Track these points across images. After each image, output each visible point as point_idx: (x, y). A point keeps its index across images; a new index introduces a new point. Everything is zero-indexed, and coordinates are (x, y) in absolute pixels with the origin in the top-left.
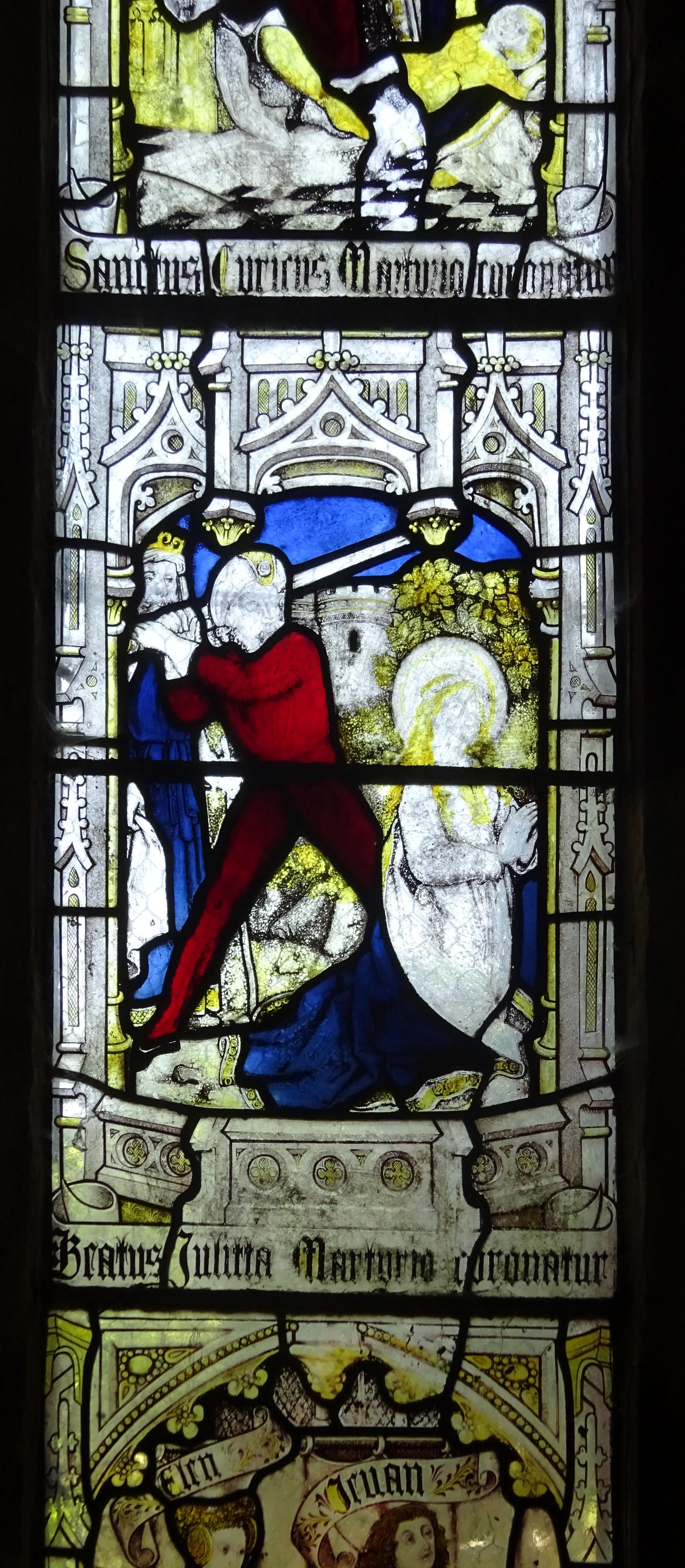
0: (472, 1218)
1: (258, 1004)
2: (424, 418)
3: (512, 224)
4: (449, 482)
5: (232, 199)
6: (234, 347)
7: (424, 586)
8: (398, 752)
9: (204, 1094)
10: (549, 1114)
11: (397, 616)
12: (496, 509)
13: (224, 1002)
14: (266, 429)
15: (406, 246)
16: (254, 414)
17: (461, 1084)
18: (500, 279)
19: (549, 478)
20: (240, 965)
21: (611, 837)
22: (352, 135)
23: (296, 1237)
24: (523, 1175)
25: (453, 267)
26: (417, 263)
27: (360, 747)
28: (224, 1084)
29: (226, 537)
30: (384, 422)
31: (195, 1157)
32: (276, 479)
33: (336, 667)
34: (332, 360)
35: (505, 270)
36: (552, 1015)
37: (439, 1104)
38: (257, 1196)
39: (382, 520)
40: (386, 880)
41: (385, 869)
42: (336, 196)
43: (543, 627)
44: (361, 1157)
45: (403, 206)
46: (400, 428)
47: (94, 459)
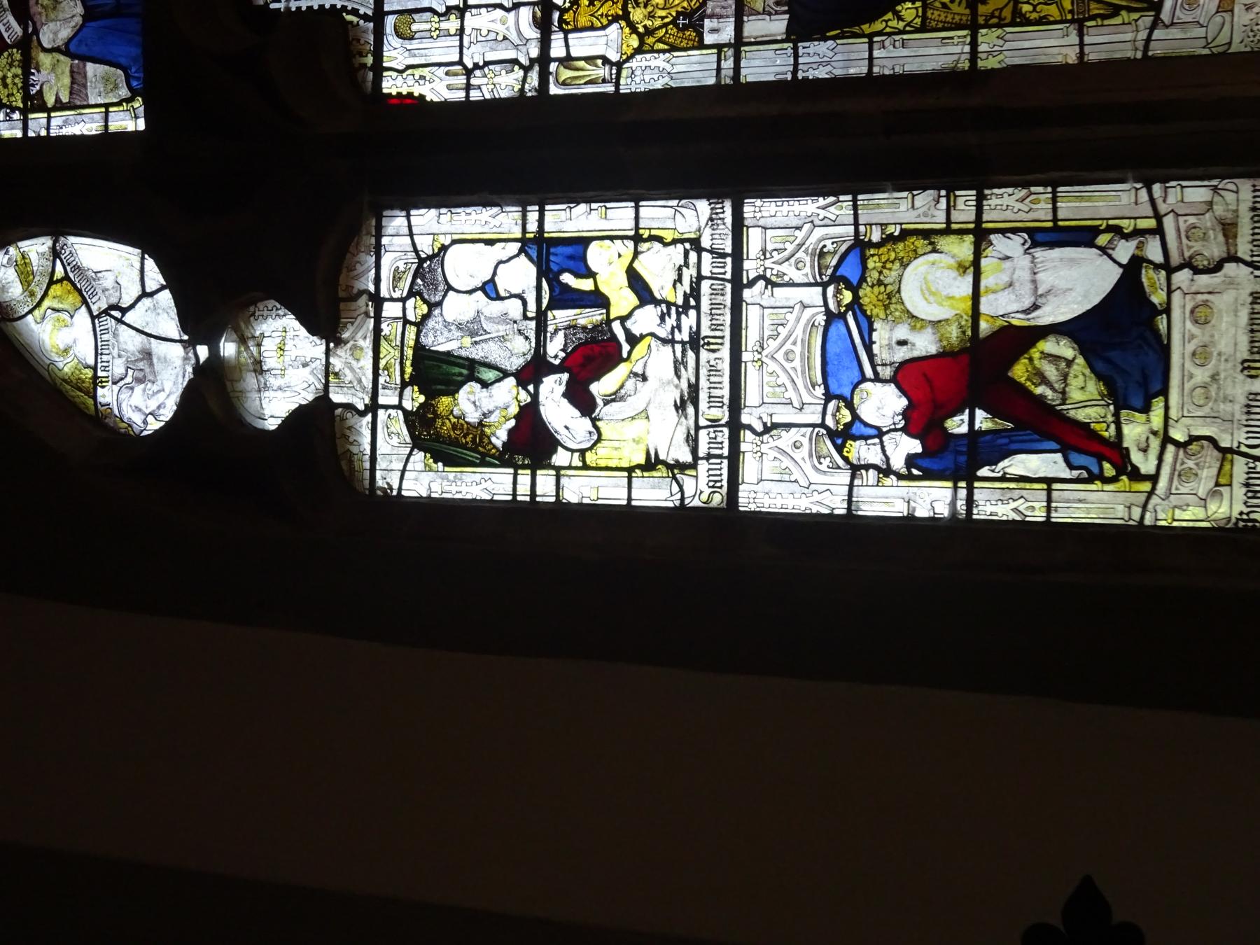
0: (1230, 268)
1: (1103, 400)
2: (787, 304)
3: (693, 256)
4: (820, 289)
5: (680, 411)
6: (750, 412)
7: (874, 303)
8: (962, 317)
9: (1155, 433)
10: (1168, 222)
11: (890, 318)
12: (834, 262)
13: (1101, 420)
14: (791, 394)
15: (703, 315)
16: (784, 401)
17: (1150, 276)
19: (819, 232)
20: (1080, 410)
21: (1010, 190)
22: (649, 345)
23: (1241, 377)
24: (1205, 237)
25: (713, 289)
26: (711, 309)
27: (959, 339)
28: (1148, 421)
29: (846, 416)
30: (788, 327)
31: (1193, 439)
32: (817, 387)
33: (916, 354)
34: (757, 356)
35: (715, 260)
36: (1111, 222)
37: (1162, 290)
38: (1216, 400)
39: (838, 327)
40: (1033, 323)
41: (1026, 324)
42: (679, 355)
43: (896, 234)
44: (1192, 337)
45: (683, 317)
46: (791, 318)
47: (806, 491)
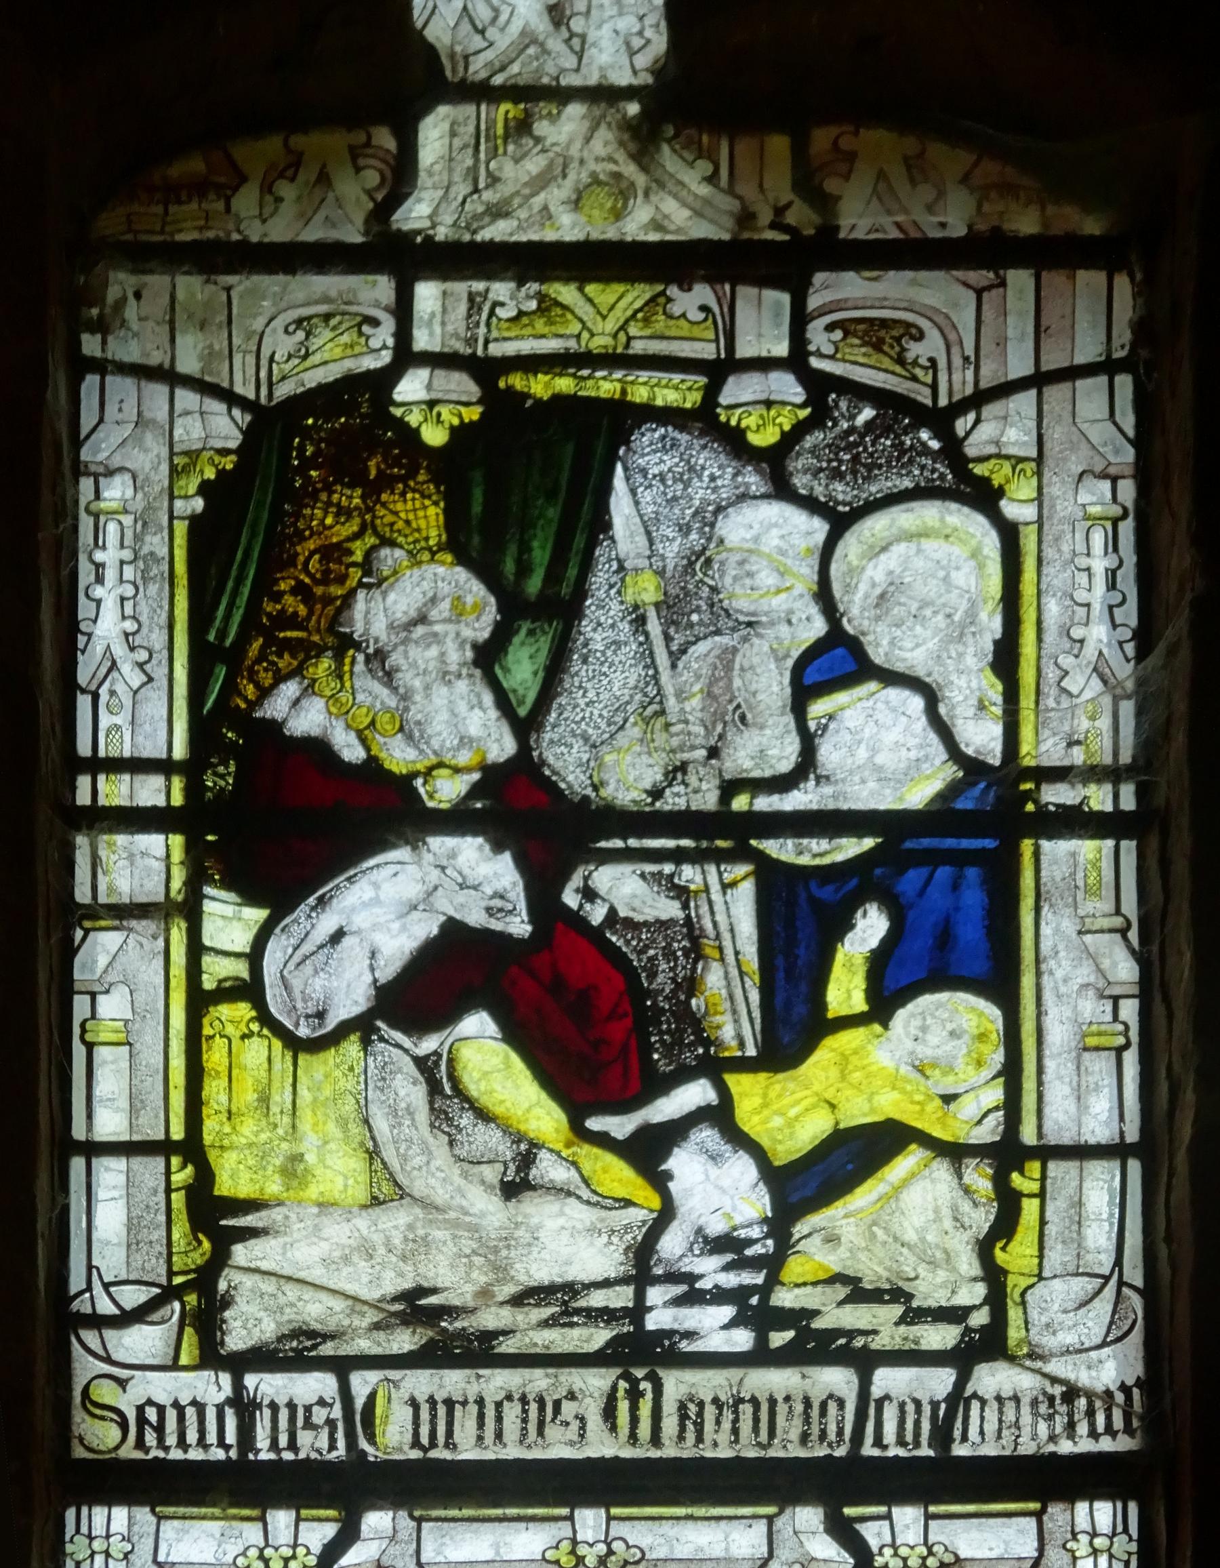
3: (940, 1337)
5: (398, 1307)
6: (403, 1535)
15: (734, 1374)
18: (917, 1423)
22: (628, 1203)
25: (824, 1406)
26: (754, 1401)
35: (927, 1410)
42: (597, 1299)
